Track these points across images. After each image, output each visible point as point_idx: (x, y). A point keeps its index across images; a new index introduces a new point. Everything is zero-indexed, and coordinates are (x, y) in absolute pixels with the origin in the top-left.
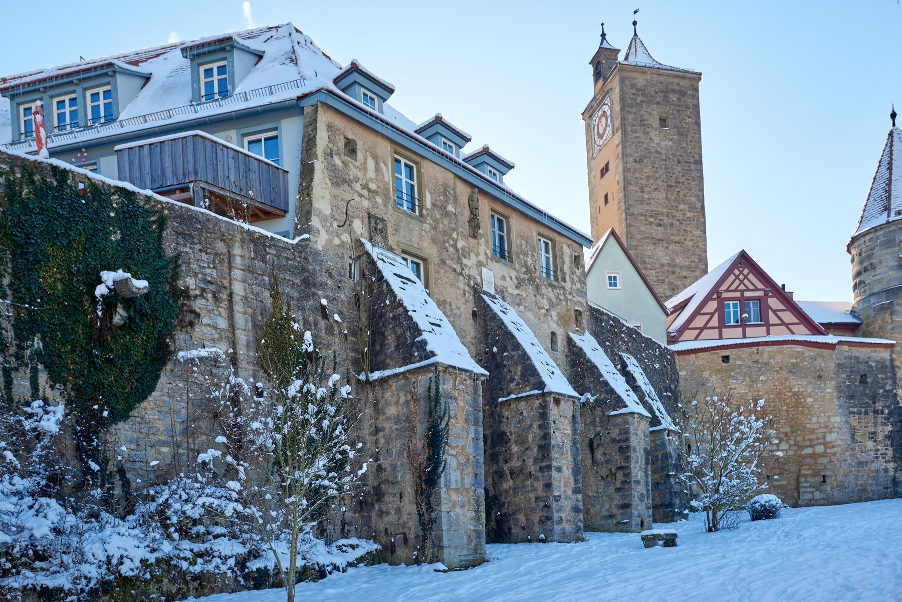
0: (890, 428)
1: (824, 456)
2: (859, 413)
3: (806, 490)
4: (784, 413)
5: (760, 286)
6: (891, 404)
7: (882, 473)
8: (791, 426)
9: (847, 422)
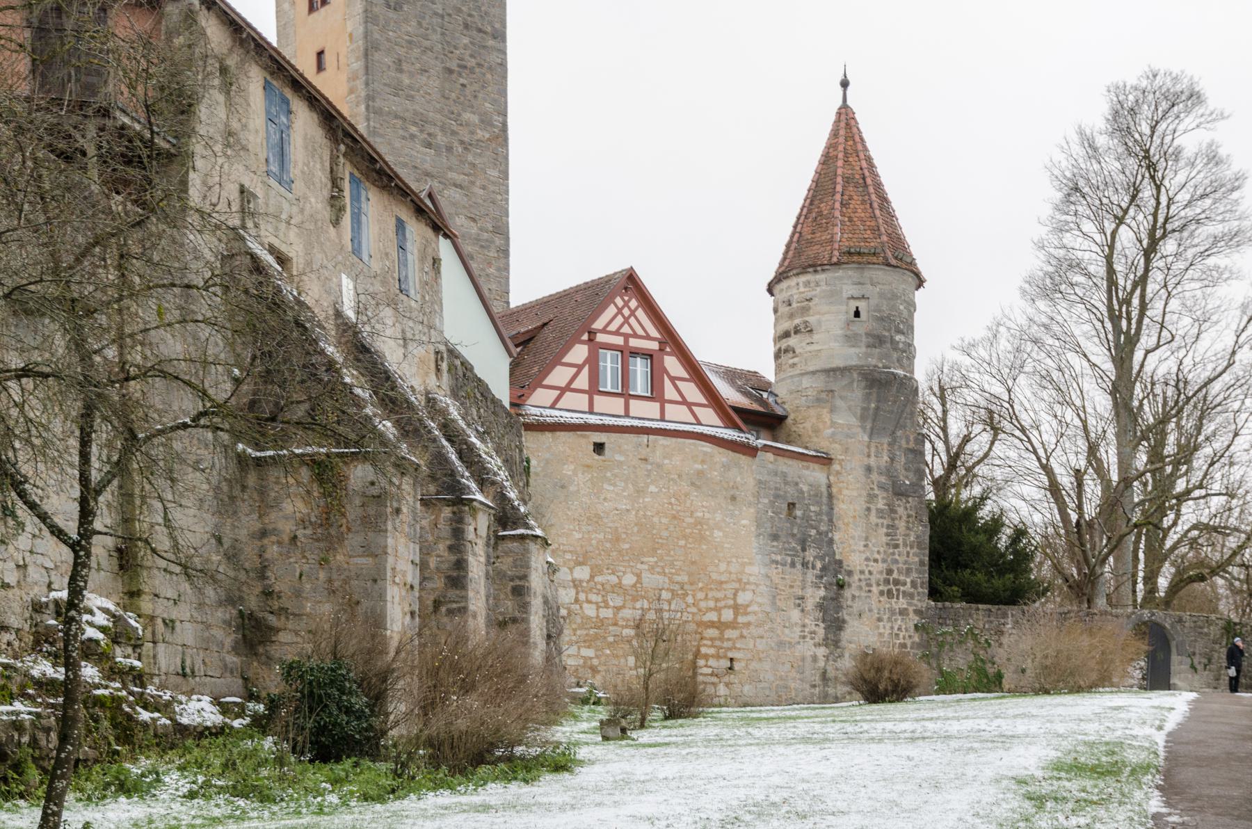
0: (822, 592)
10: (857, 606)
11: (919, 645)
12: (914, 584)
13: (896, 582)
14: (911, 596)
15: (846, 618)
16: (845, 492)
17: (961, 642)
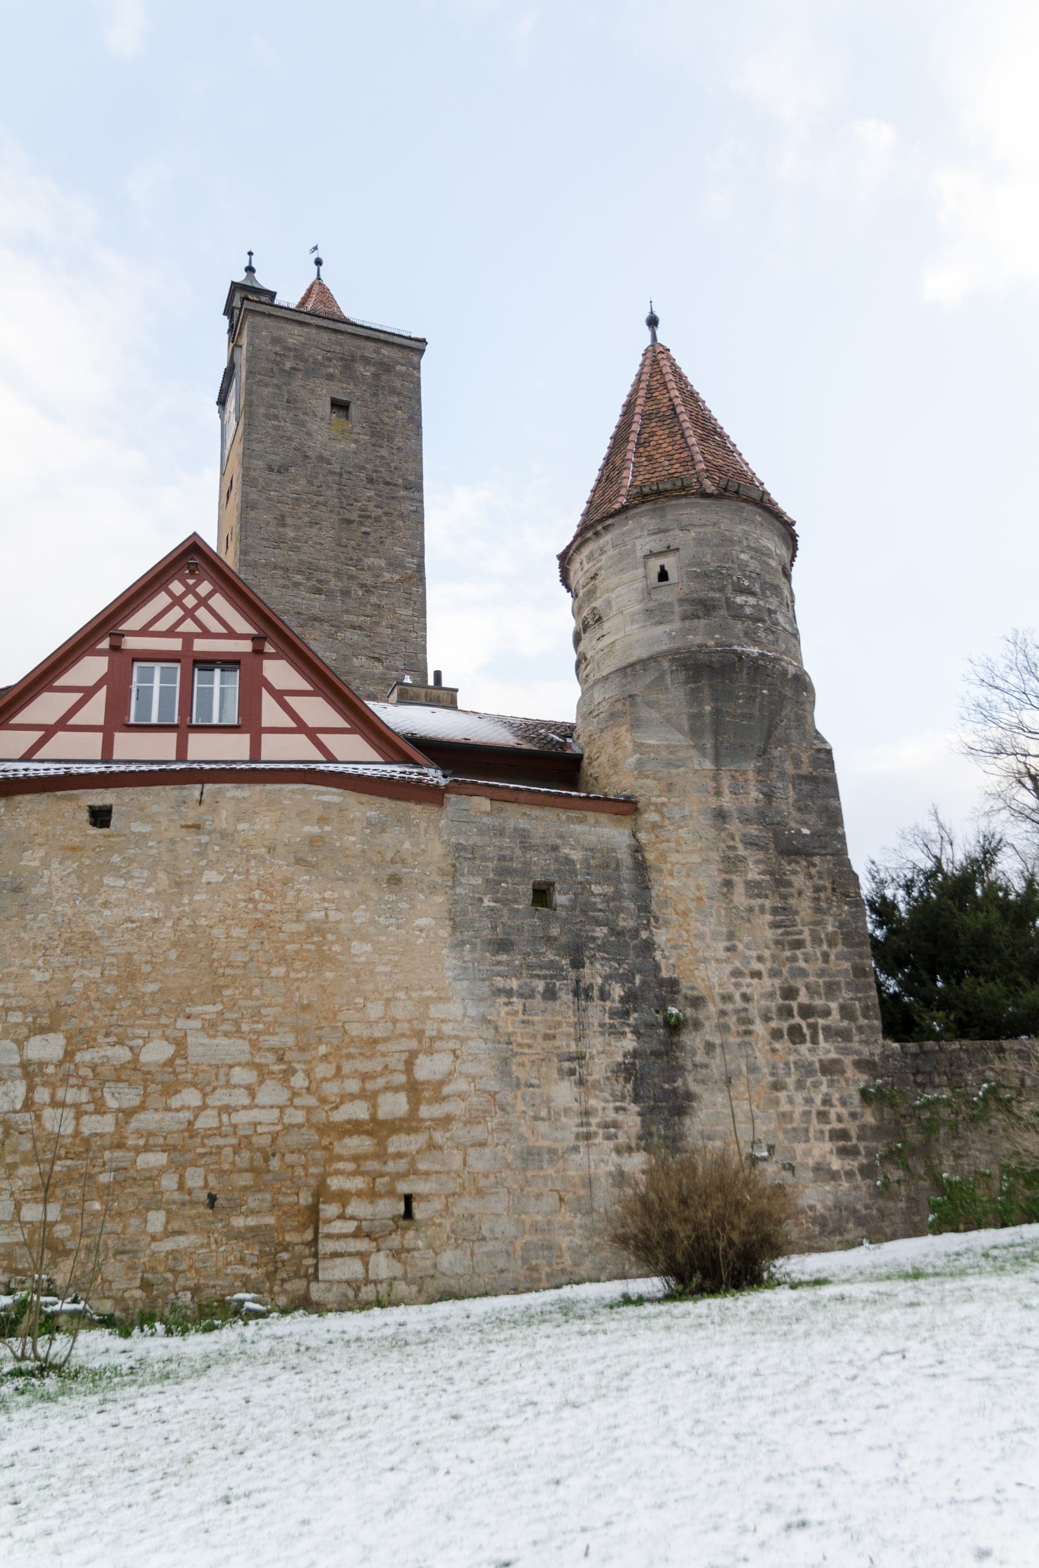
0: (629, 1043)
5: (241, 625)
11: (878, 1132)
12: (846, 1012)
13: (807, 1011)
14: (845, 1035)
15: (694, 1088)
16: (674, 857)
17: (973, 1119)
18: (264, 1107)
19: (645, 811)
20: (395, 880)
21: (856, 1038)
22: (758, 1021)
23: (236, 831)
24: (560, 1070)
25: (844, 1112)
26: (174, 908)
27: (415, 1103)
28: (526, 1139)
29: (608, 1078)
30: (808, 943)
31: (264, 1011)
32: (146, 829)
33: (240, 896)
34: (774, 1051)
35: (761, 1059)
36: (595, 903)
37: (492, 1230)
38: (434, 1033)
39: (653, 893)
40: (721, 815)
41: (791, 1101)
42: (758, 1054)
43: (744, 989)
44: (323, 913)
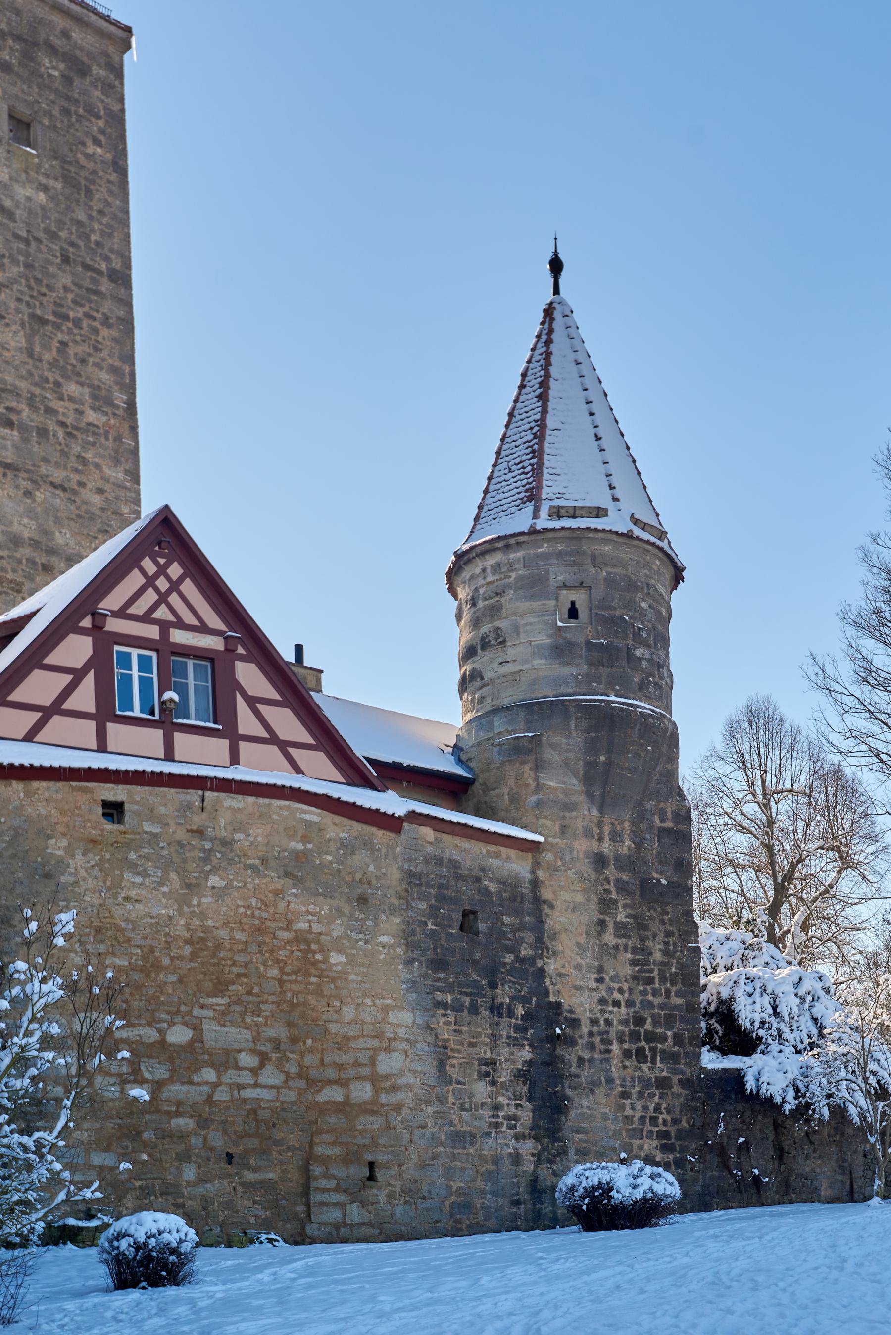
0: (526, 1054)
1: (373, 1112)
2: (457, 1008)
3: (325, 1197)
4: (273, 986)
6: (531, 993)
7: (507, 1166)
8: (290, 1025)
9: (428, 1028)
10: (586, 1073)
13: (651, 1037)
15: (569, 1092)
18: (265, 1087)
19: (543, 850)
20: (363, 900)
21: (683, 1061)
22: (615, 1042)
23: (233, 840)
24: (479, 1072)
25: (668, 1118)
26: (186, 909)
27: (377, 1091)
28: (455, 1125)
29: (511, 1081)
30: (657, 981)
31: (263, 1007)
32: (156, 830)
33: (239, 903)
34: (625, 1067)
35: (615, 1073)
36: (505, 933)
37: (430, 1192)
38: (392, 1036)
39: (546, 927)
40: (600, 861)
41: (633, 1108)
42: (613, 1069)
43: (607, 1015)
44: (307, 925)
